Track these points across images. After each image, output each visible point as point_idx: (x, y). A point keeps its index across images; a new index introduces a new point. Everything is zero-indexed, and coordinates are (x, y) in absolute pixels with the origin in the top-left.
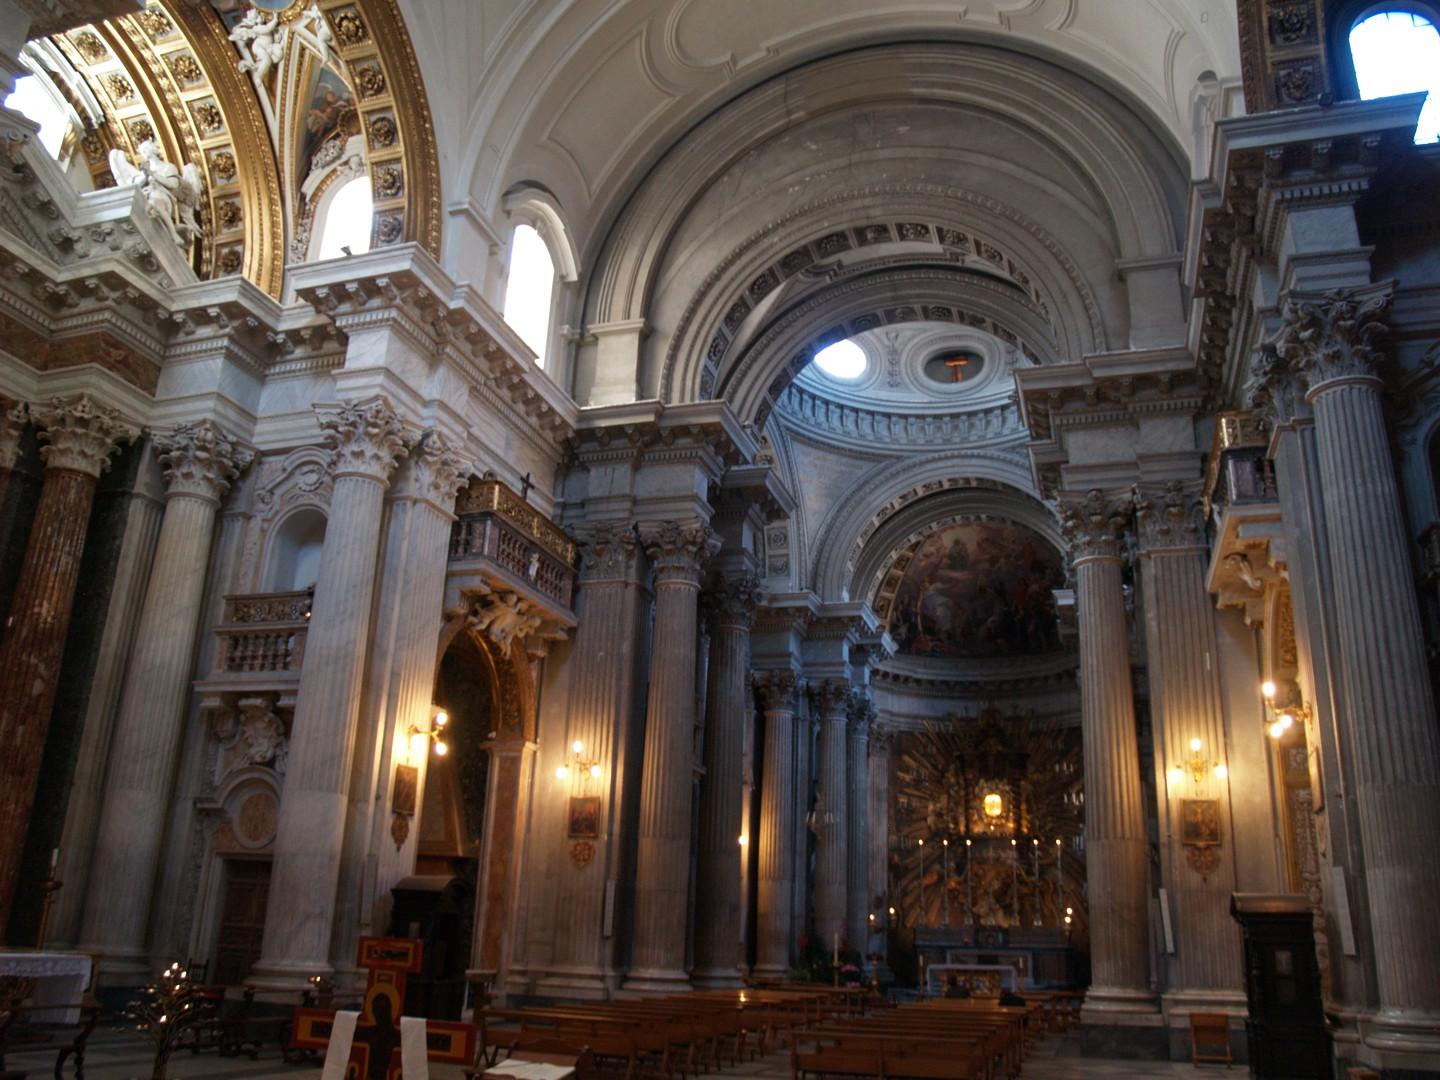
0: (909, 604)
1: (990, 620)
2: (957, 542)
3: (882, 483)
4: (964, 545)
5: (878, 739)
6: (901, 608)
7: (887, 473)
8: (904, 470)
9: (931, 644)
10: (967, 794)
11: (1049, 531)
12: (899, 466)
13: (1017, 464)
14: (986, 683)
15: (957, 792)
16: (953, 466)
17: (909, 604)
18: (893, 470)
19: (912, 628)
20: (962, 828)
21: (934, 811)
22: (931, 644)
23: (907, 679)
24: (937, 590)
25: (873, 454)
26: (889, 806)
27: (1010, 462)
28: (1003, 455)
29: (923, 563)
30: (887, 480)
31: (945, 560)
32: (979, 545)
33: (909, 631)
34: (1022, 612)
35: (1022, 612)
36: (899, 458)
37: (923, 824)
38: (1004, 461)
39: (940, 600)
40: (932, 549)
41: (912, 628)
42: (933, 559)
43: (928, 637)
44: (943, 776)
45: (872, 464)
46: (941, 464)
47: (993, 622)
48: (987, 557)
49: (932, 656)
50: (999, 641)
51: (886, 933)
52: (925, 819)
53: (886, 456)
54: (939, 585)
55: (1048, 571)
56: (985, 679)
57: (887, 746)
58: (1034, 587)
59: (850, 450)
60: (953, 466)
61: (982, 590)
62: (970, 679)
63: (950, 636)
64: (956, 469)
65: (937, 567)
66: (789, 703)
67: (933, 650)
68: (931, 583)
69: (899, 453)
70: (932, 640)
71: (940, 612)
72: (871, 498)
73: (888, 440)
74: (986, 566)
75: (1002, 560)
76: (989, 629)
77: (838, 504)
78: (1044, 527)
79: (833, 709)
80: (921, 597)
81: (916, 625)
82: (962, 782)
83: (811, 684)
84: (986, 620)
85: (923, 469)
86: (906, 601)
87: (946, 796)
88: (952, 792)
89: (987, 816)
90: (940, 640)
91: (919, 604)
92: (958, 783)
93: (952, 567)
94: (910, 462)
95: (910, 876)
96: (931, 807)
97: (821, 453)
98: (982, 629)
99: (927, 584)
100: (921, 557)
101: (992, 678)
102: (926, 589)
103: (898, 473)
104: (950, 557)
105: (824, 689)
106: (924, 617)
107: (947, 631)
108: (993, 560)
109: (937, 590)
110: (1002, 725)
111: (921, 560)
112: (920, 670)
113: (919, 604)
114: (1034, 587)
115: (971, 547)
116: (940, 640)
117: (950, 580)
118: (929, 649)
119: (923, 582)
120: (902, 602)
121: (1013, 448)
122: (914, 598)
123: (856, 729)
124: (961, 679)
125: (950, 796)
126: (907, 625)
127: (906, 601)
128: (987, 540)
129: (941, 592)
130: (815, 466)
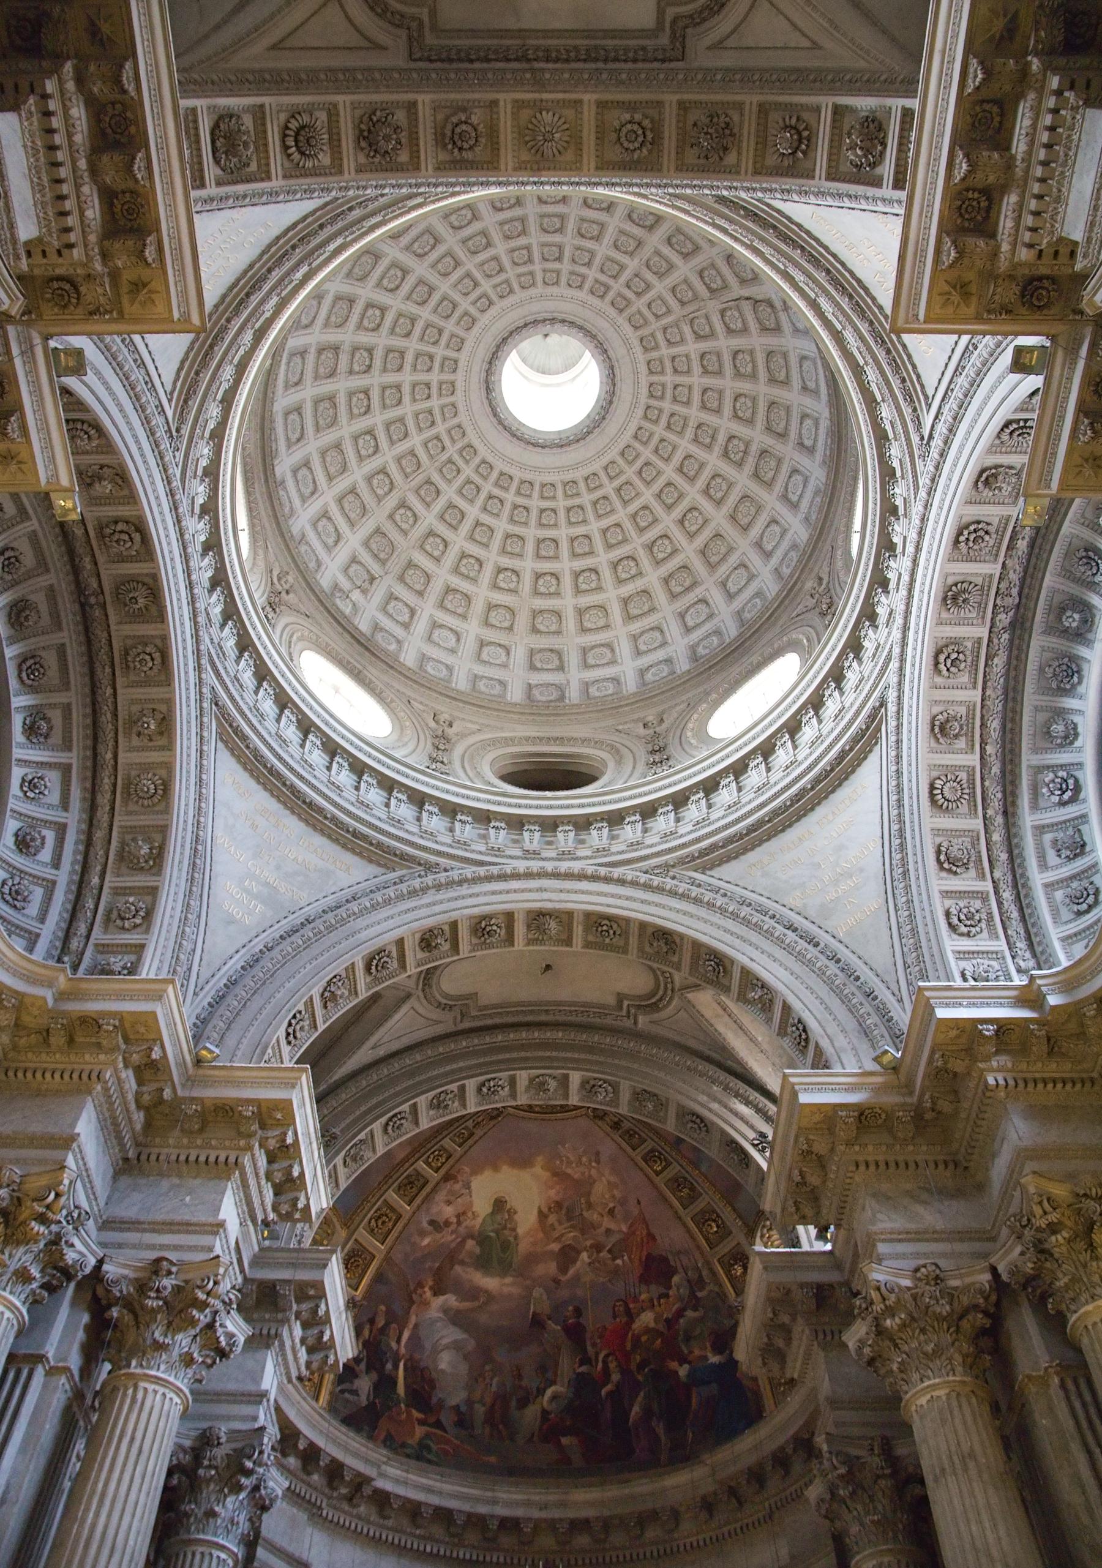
0: (383, 1330)
1: (549, 1392)
2: (499, 1204)
3: (388, 902)
4: (512, 1212)
6: (366, 1333)
7: (404, 887)
8: (438, 887)
9: (420, 1431)
11: (715, 1106)
12: (429, 879)
13: (673, 893)
14: (538, 1524)
16: (540, 890)
17: (383, 1330)
18: (416, 883)
19: (385, 1384)
22: (420, 1431)
23: (361, 1482)
24: (446, 1310)
25: (379, 845)
27: (660, 890)
28: (643, 878)
29: (426, 1241)
30: (401, 897)
31: (470, 1244)
32: (542, 1216)
33: (377, 1387)
34: (616, 1377)
35: (616, 1377)
36: (429, 867)
38: (647, 887)
39: (451, 1334)
40: (449, 1212)
41: (385, 1384)
42: (447, 1237)
43: (416, 1414)
45: (373, 869)
46: (515, 884)
47: (554, 1397)
48: (555, 1247)
49: (419, 1458)
50: (565, 1441)
53: (403, 857)
54: (451, 1300)
55: (676, 1279)
56: (536, 1514)
58: (647, 1319)
59: (334, 819)
60: (540, 890)
61: (537, 1322)
62: (501, 1511)
63: (463, 1421)
64: (545, 895)
65: (451, 1257)
66: (23, 1276)
67: (423, 1446)
68: (437, 1292)
69: (433, 859)
70: (422, 1423)
71: (445, 1362)
72: (361, 923)
73: (415, 829)
74: (552, 1268)
75: (584, 1256)
76: (545, 1413)
77: (285, 925)
78: (703, 1098)
79: (160, 1347)
80: (413, 1319)
83: (110, 1270)
84: (541, 1392)
85: (477, 889)
86: (380, 1322)
90: (438, 1425)
91: (406, 1335)
93: (483, 1263)
94: (455, 875)
97: (273, 805)
98: (532, 1412)
99: (428, 1294)
100: (425, 1225)
101: (556, 1514)
102: (426, 1304)
103: (425, 890)
104: (482, 1239)
105: (142, 1287)
107: (457, 1408)
108: (567, 1255)
109: (446, 1310)
111: (422, 1234)
112: (393, 1471)
113: (406, 1335)
114: (647, 1319)
115: (526, 1221)
116: (438, 1425)
117: (472, 1293)
118: (413, 1441)
119: (420, 1285)
120: (372, 1321)
121: (667, 866)
122: (396, 1319)
123: (211, 1514)
124: (482, 1509)
126: (374, 1376)
127: (380, 1322)
128: (559, 1205)
129: (456, 1318)
130: (254, 827)
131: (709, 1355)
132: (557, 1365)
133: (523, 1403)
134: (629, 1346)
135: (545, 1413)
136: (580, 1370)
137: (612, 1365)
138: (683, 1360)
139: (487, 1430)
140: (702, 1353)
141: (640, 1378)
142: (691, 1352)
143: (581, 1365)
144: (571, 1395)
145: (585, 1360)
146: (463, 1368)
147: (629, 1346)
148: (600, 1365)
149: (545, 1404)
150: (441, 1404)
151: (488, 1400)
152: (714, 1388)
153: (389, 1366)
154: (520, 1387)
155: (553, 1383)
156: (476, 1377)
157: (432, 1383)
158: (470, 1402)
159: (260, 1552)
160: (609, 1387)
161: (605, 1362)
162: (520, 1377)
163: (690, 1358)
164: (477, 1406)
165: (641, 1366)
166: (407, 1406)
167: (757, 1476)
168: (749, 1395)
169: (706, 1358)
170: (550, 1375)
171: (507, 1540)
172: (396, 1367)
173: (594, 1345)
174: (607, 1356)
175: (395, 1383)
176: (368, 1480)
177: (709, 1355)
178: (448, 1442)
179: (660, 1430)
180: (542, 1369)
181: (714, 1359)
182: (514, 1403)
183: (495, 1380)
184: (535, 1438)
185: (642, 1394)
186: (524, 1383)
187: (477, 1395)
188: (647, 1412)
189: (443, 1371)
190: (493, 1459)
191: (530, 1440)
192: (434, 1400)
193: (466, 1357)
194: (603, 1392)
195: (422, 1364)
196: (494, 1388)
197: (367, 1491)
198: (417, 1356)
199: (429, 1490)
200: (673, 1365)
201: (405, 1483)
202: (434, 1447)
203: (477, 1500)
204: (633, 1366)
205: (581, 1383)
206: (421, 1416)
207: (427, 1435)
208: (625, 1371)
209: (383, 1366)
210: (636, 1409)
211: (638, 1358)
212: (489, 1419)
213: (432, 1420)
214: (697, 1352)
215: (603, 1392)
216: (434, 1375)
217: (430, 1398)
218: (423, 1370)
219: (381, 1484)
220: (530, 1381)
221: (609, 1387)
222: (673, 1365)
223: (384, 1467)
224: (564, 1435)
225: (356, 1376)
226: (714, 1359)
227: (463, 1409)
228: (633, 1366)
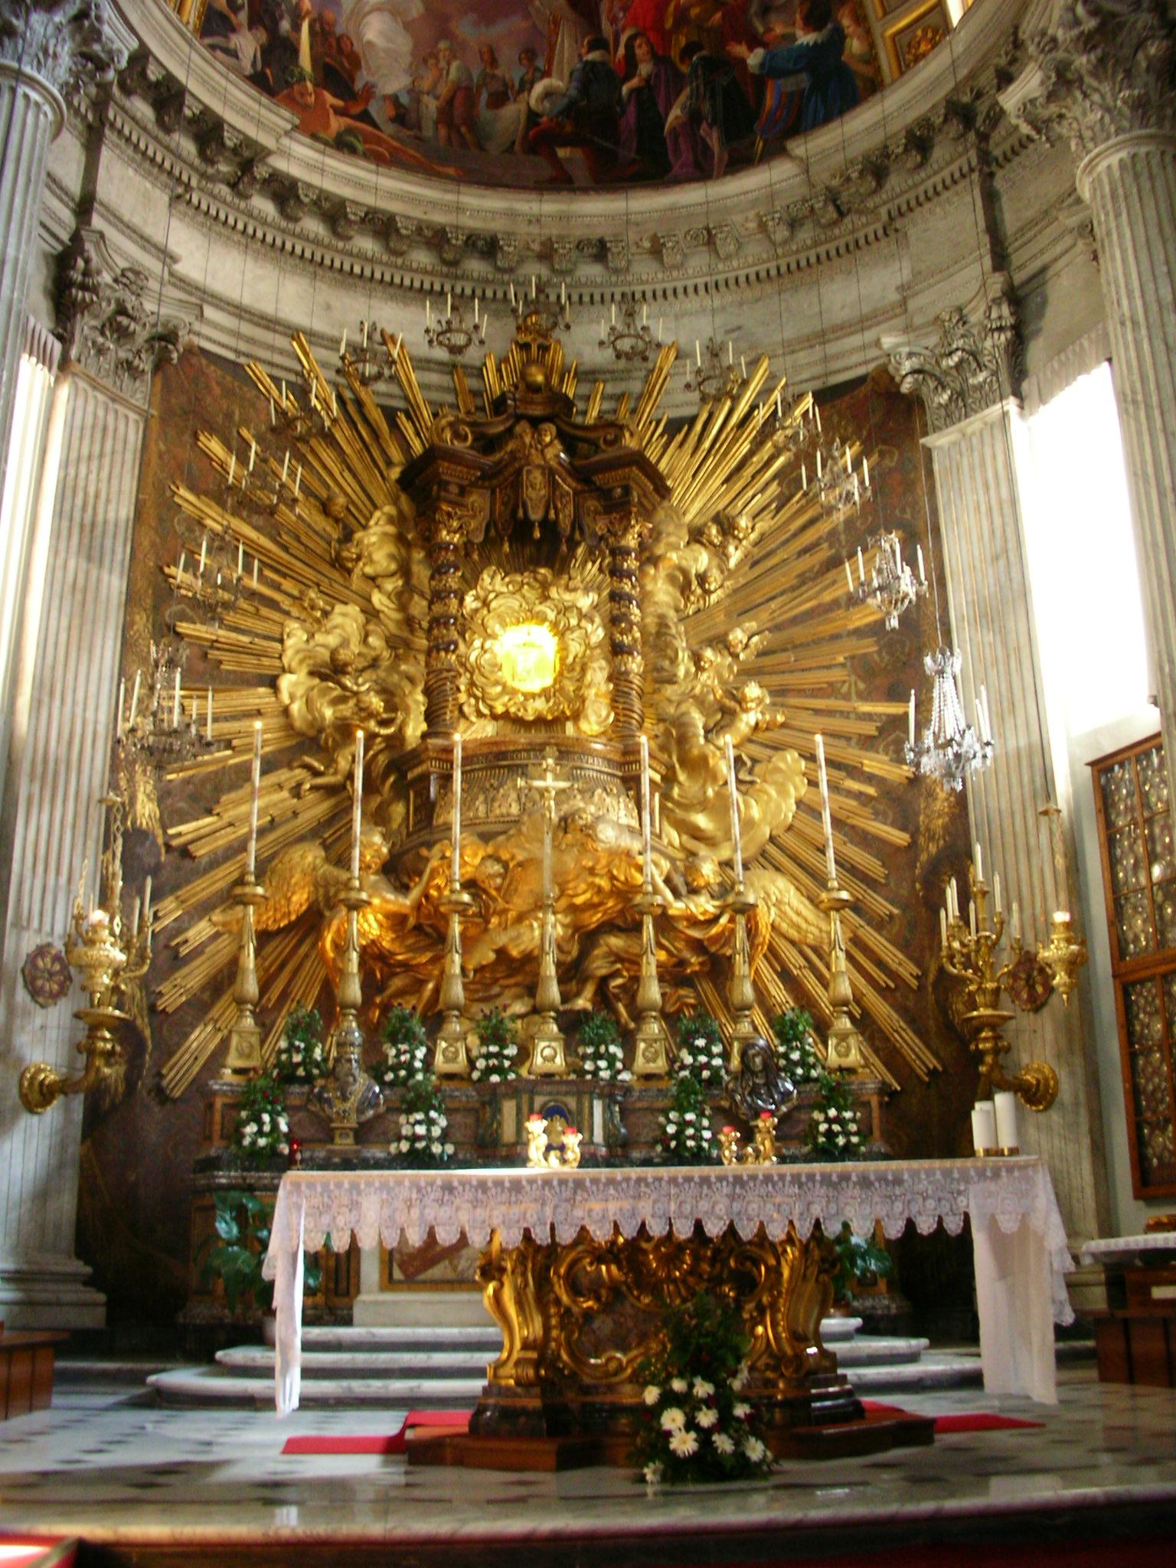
1: (539, 88)
5: (123, 334)
9: (336, 124)
10: (438, 622)
15: (402, 599)
20: (415, 729)
21: (307, 655)
22: (336, 124)
26: (131, 599)
34: (645, 69)
37: (260, 696)
43: (330, 99)
44: (347, 537)
47: (548, 94)
50: (562, 153)
51: (78, 1104)
52: (272, 683)
57: (146, 364)
62: (469, 222)
63: (402, 116)
70: (340, 112)
76: (532, 116)
81: (291, 49)
82: (421, 572)
84: (526, 85)
87: (353, 610)
88: (378, 599)
89: (508, 691)
90: (365, 117)
92: (404, 570)
95: (204, 888)
96: (296, 636)
98: (512, 113)
106: (323, 33)
107: (394, 99)
110: (570, 390)
124: (439, 218)
125: (371, 614)
126: (262, 36)
131: (799, 33)
132: (552, 48)
133: (499, 100)
134: (669, 23)
135: (532, 116)
136: (590, 57)
137: (641, 51)
138: (754, 42)
139: (443, 132)
140: (789, 30)
141: (685, 69)
142: (769, 30)
143: (589, 51)
144: (573, 92)
145: (598, 43)
146: (404, 44)
147: (669, 23)
148: (621, 51)
149: (533, 102)
150: (369, 91)
151: (443, 90)
152: (804, 80)
153: (285, 25)
154: (494, 76)
155: (547, 74)
156: (424, 56)
157: (355, 61)
158: (414, 92)
159: (97, 222)
160: (634, 82)
161: (629, 46)
162: (493, 62)
163: (768, 38)
164: (426, 99)
165: (687, 52)
166: (316, 85)
167: (877, 168)
168: (859, 83)
169: (793, 38)
170: (540, 63)
171: (476, 266)
172: (297, 28)
173: (613, 21)
174: (631, 39)
175: (295, 51)
176: (263, 152)
177: (799, 33)
178: (379, 141)
179: (714, 140)
180: (529, 54)
181: (806, 38)
182: (484, 97)
183: (455, 65)
184: (517, 147)
185: (687, 91)
186: (499, 72)
187: (426, 85)
188: (694, 117)
189: (369, 43)
190: (451, 171)
191: (510, 149)
192: (359, 85)
193: (408, 26)
194: (625, 89)
195: (339, 30)
196: (453, 73)
197: (261, 172)
198: (329, 15)
199: (360, 185)
200: (740, 50)
201: (322, 171)
202: (360, 147)
203: (433, 204)
204: (675, 54)
205: (591, 77)
206: (339, 103)
207: (349, 131)
208: (660, 59)
209: (276, 23)
210: (675, 113)
211: (683, 41)
212: (446, 114)
213: (356, 110)
214: (779, 30)
215: (625, 89)
216: (357, 48)
217: (352, 79)
218: (339, 39)
219: (280, 164)
220: (511, 70)
221: (634, 82)
222: (740, 50)
223: (286, 141)
224: (564, 145)
225: (234, 30)
226: (806, 38)
227: (404, 100)
228: (675, 54)
